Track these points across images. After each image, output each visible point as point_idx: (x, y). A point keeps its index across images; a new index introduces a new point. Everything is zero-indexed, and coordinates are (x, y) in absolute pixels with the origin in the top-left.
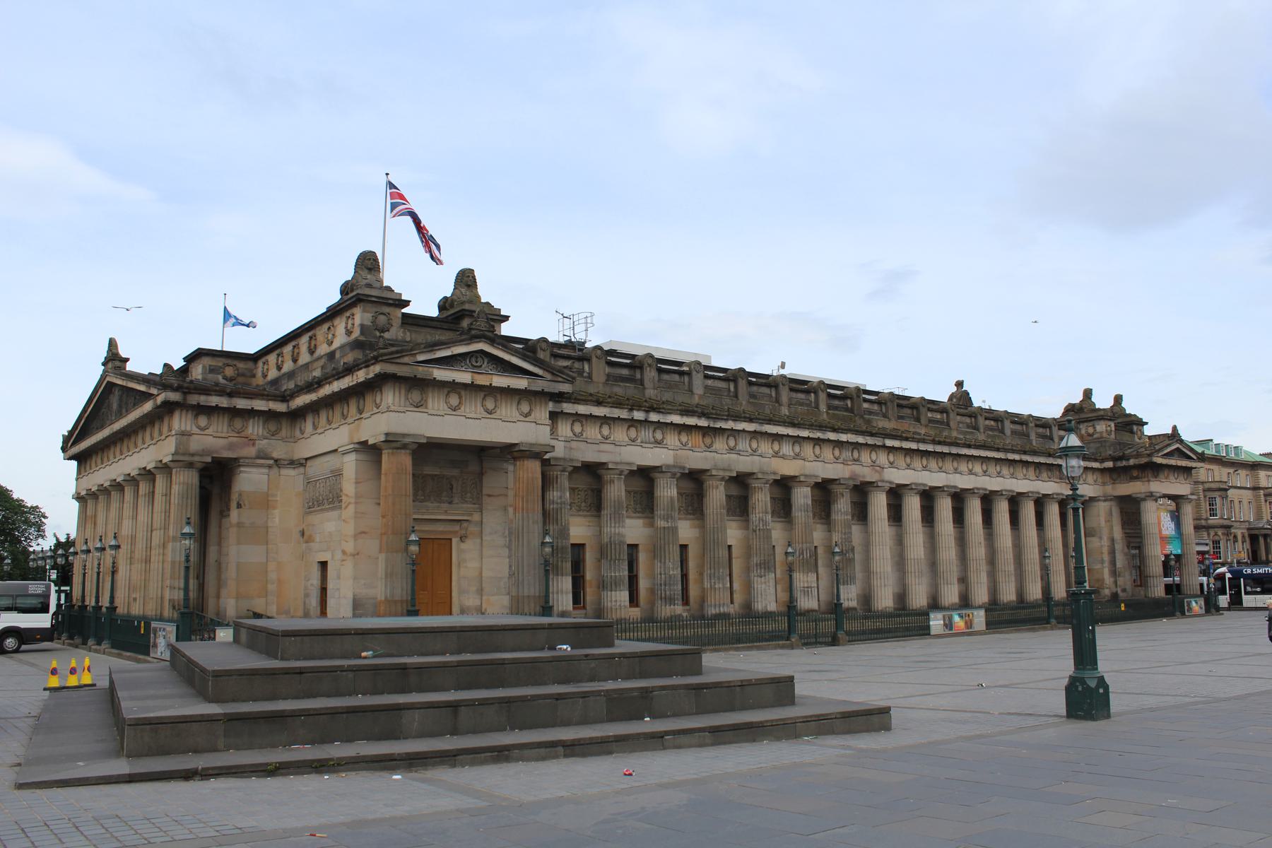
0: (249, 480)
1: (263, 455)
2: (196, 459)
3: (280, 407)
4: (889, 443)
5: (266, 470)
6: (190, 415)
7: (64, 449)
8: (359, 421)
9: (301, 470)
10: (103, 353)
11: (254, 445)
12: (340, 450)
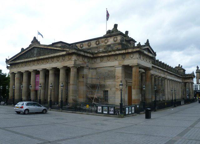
0: (86, 71)
1: (87, 66)
2: (78, 66)
3: (91, 56)
4: (168, 71)
5: (87, 70)
6: (76, 56)
7: (6, 62)
9: (95, 70)
10: (32, 39)
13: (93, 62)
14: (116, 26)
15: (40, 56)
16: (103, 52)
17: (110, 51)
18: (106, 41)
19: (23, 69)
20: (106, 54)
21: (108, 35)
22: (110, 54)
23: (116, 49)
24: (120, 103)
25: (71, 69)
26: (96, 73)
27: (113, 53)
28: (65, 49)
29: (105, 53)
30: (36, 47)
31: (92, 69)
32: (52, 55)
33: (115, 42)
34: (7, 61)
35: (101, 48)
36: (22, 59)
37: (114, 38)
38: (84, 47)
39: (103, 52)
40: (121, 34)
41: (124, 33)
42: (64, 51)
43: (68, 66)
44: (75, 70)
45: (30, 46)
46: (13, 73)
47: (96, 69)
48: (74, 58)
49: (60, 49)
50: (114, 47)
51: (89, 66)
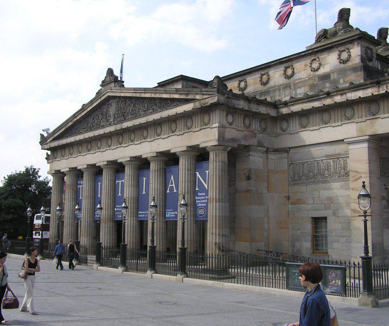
0: (256, 160)
1: (260, 145)
2: (230, 144)
3: (273, 113)
5: (261, 155)
7: (42, 143)
8: (373, 120)
9: (285, 155)
11: (256, 137)
12: (345, 141)
13: (279, 131)
14: (344, 14)
15: (125, 120)
16: (308, 98)
17: (328, 95)
18: (315, 65)
19: (82, 160)
20: (317, 104)
21: (318, 45)
22: (328, 102)
23: (347, 85)
24: (363, 255)
25: (211, 156)
26: (289, 165)
27: (338, 99)
28: (190, 97)
29: (310, 101)
30: (114, 97)
31: (277, 151)
32: (156, 116)
33: (342, 65)
34: (43, 141)
35: (300, 88)
36: (80, 133)
37: (341, 52)
38: (249, 90)
39: (308, 98)
40: (363, 37)
41: (375, 34)
42: (187, 101)
43: (202, 145)
44: (224, 156)
45: (99, 93)
46: (59, 171)
47: (287, 150)
48: (216, 120)
49: (176, 96)
50: (341, 81)
51: (266, 145)
